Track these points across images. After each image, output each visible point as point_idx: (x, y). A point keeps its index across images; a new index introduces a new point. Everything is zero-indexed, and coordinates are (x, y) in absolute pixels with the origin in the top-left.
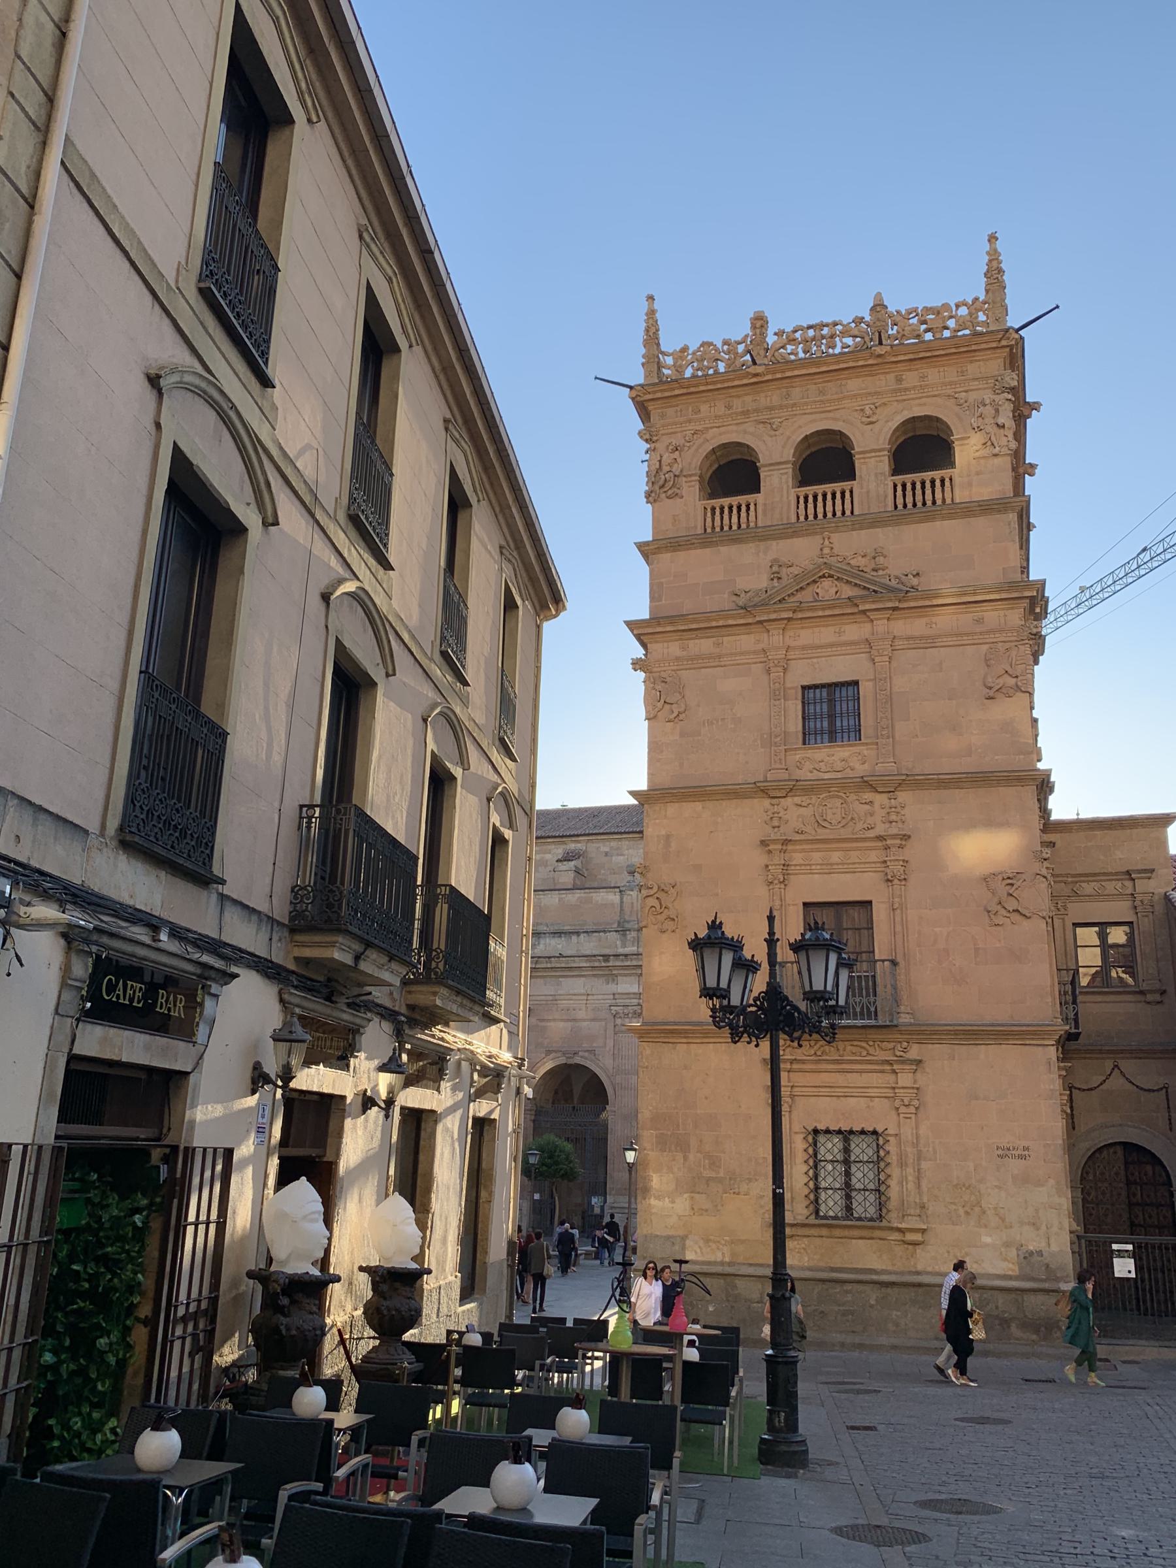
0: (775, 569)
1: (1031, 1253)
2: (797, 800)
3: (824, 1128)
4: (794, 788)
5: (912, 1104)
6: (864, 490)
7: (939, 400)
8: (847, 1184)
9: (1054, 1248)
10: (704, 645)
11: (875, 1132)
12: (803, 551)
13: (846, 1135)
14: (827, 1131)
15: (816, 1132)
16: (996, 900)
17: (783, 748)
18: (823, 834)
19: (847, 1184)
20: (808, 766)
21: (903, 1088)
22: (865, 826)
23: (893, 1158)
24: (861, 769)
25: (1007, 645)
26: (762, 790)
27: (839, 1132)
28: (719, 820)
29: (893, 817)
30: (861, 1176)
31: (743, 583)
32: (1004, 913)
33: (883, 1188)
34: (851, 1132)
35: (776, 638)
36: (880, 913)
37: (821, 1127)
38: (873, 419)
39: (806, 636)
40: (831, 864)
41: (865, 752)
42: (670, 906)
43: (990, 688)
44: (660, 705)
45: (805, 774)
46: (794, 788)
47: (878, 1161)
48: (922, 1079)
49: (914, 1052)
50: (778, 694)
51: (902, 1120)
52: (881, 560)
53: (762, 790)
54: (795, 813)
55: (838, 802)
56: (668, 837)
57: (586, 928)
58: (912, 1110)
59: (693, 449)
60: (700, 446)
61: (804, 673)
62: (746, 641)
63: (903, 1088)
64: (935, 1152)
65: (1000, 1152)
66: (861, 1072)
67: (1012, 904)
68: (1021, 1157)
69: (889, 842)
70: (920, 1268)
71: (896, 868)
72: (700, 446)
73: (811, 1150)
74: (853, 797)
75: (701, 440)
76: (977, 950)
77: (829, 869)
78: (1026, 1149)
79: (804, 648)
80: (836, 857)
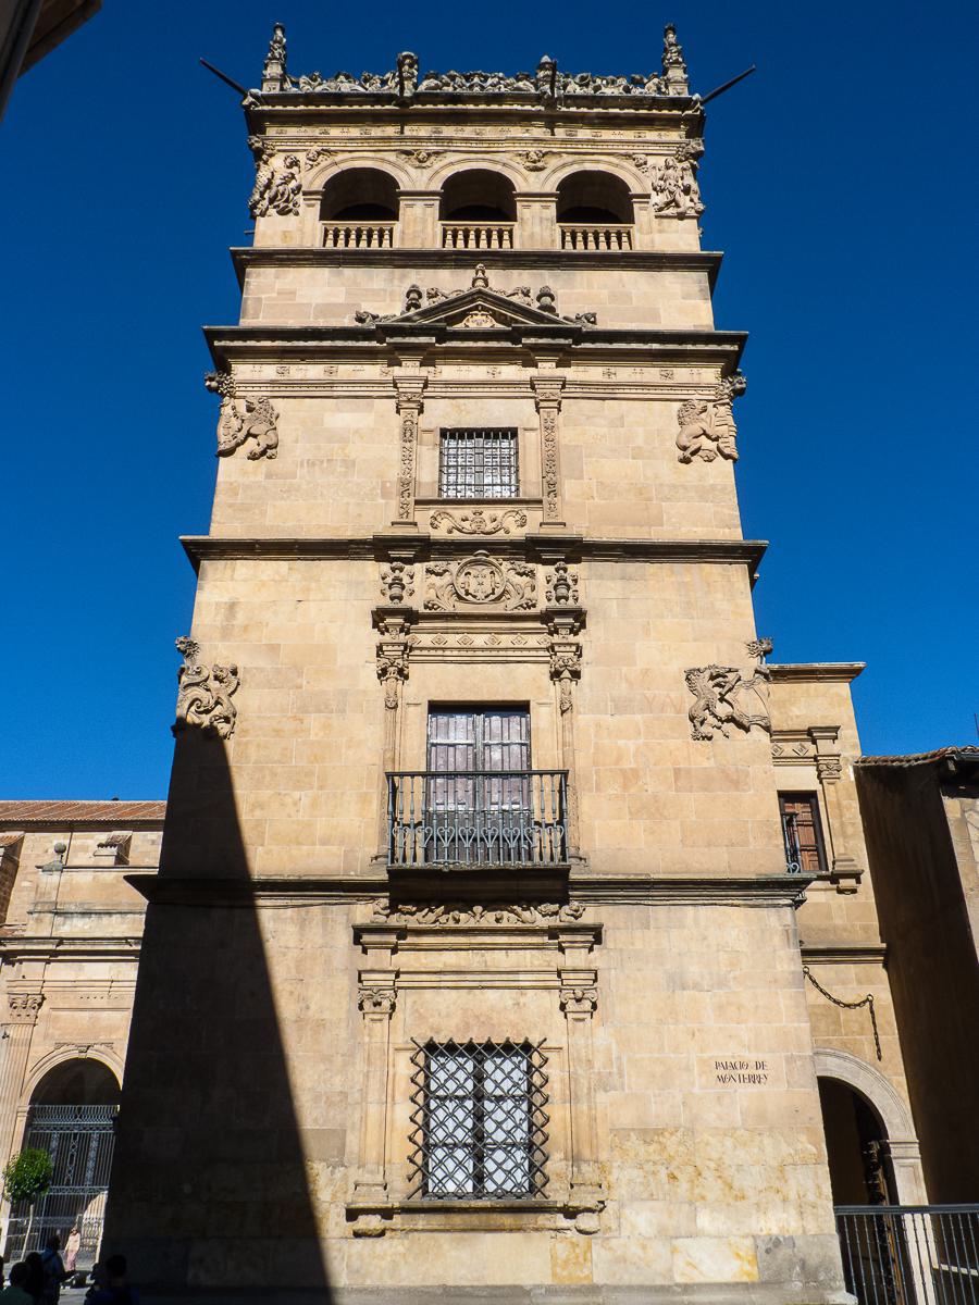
0: (413, 295)
1: (777, 1243)
2: (431, 564)
3: (445, 1041)
4: (425, 549)
5: (581, 999)
6: (526, 234)
7: (611, 159)
8: (479, 1135)
9: (812, 1228)
10: (314, 371)
11: (527, 1048)
12: (452, 282)
13: (479, 1052)
14: (451, 1049)
15: (431, 1048)
16: (702, 703)
17: (412, 500)
18: (462, 608)
19: (479, 1135)
20: (445, 524)
21: (575, 971)
22: (523, 602)
23: (555, 1089)
24: (517, 533)
25: (703, 403)
26: (379, 548)
27: (470, 1048)
28: (313, 585)
29: (562, 591)
30: (503, 1123)
31: (369, 307)
32: (711, 720)
33: (538, 1138)
34: (489, 1047)
35: (410, 369)
36: (543, 716)
37: (441, 1039)
38: (539, 165)
39: (448, 371)
40: (474, 649)
41: (525, 512)
42: (224, 698)
43: (684, 448)
44: (241, 436)
45: (440, 534)
46: (425, 549)
47: (532, 1096)
48: (597, 958)
49: (590, 915)
50: (408, 434)
51: (570, 1026)
52: (546, 300)
53: (379, 548)
54: (423, 585)
55: (487, 571)
56: (232, 607)
57: (120, 909)
58: (587, 1005)
59: (316, 169)
60: (326, 168)
61: (441, 413)
62: (372, 371)
63: (575, 971)
64: (621, 1075)
65: (721, 1072)
66: (509, 948)
67: (722, 710)
68: (753, 1079)
69: (556, 620)
70: (598, 1279)
71: (566, 654)
72: (326, 168)
73: (421, 1079)
74: (506, 565)
75: (329, 161)
76: (677, 772)
77: (469, 656)
78: (760, 1065)
79: (447, 384)
80: (480, 640)
